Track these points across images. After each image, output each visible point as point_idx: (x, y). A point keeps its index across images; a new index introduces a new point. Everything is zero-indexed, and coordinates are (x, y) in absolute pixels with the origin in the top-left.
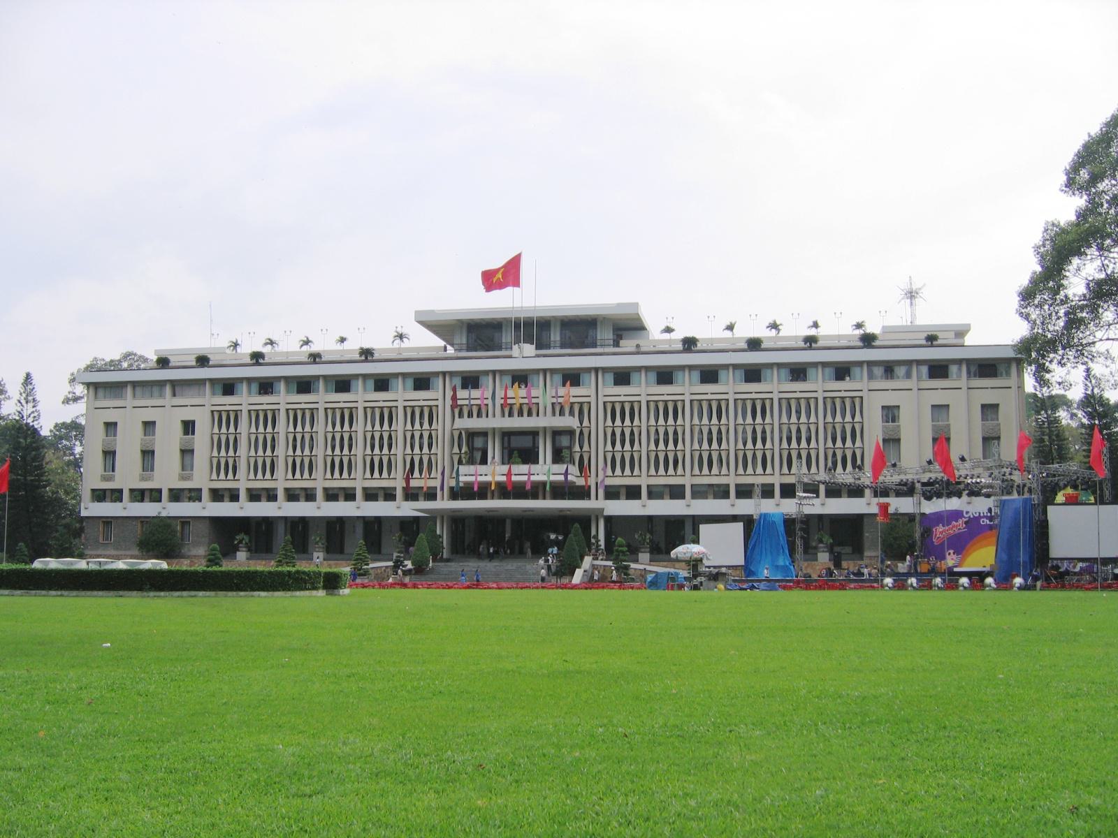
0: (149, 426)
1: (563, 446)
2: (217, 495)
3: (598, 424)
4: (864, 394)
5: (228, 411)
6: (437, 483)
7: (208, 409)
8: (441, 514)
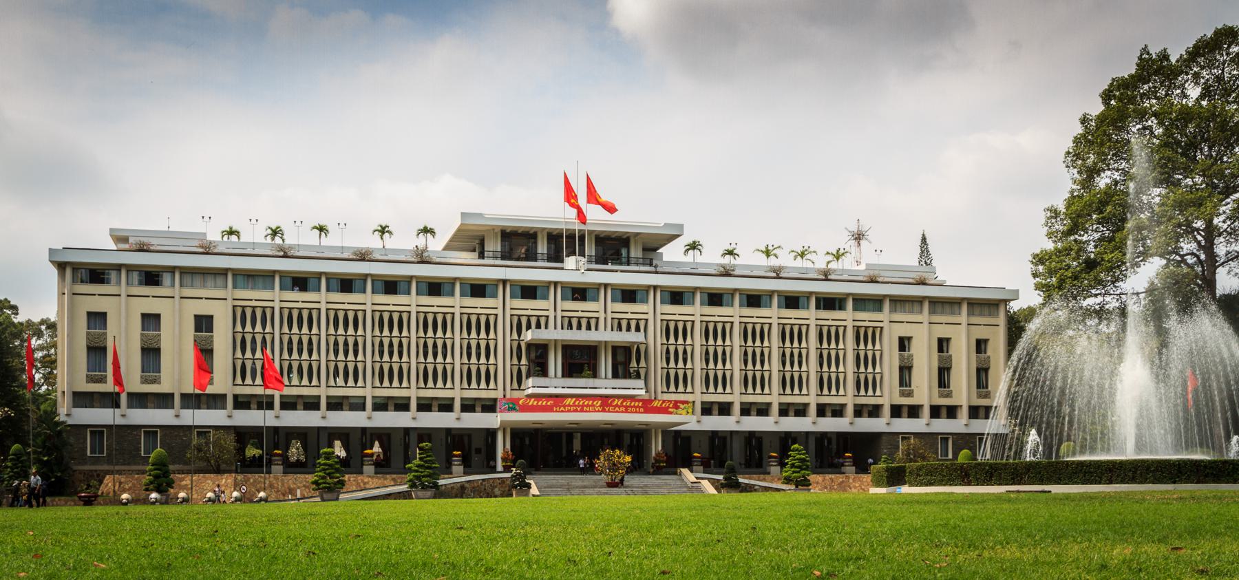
0: (150, 320)
1: (625, 361)
2: (242, 403)
3: (654, 340)
4: (885, 325)
5: (254, 307)
6: (498, 394)
7: (230, 303)
8: (504, 426)
